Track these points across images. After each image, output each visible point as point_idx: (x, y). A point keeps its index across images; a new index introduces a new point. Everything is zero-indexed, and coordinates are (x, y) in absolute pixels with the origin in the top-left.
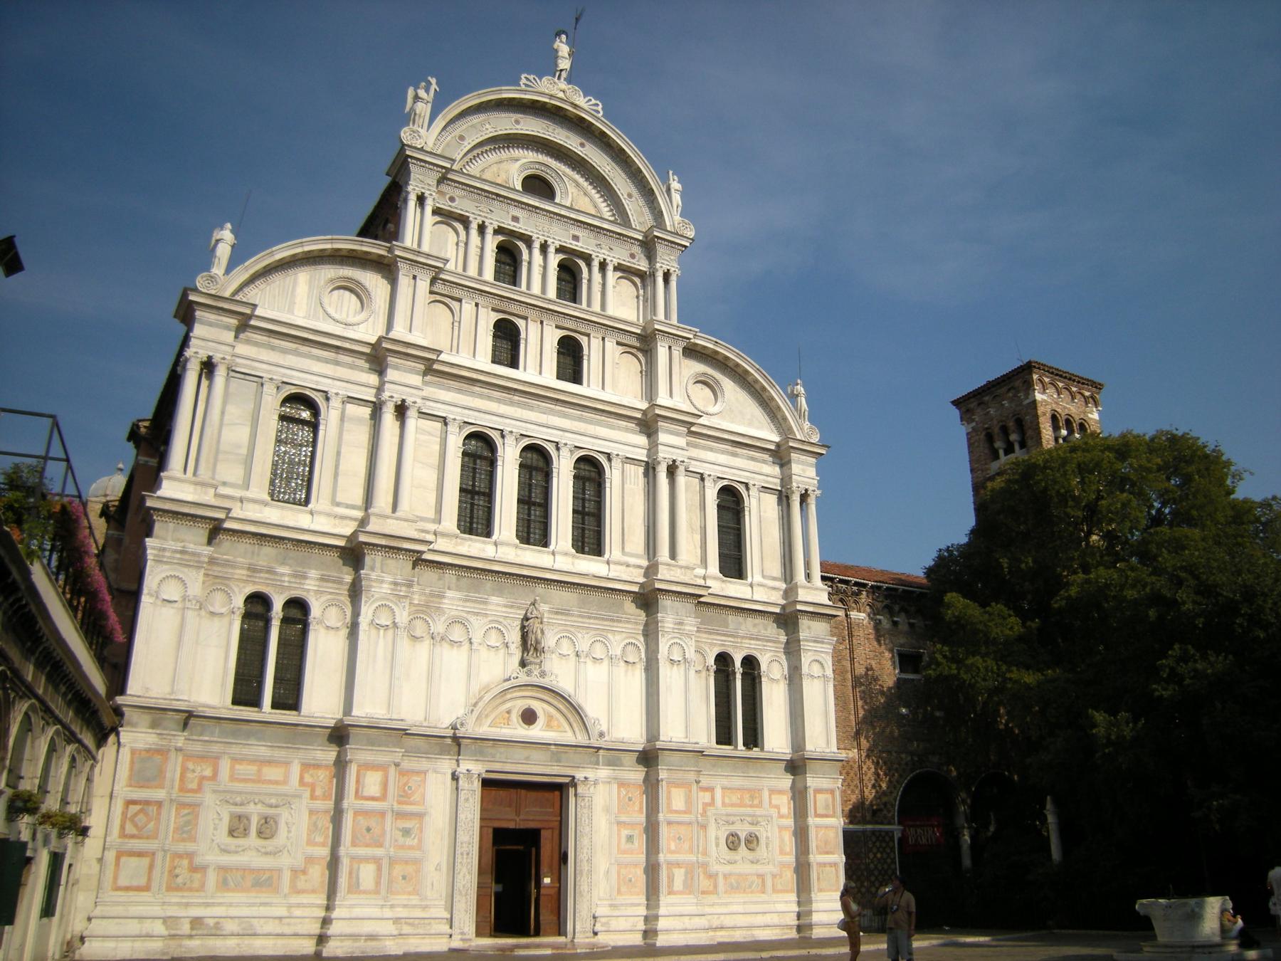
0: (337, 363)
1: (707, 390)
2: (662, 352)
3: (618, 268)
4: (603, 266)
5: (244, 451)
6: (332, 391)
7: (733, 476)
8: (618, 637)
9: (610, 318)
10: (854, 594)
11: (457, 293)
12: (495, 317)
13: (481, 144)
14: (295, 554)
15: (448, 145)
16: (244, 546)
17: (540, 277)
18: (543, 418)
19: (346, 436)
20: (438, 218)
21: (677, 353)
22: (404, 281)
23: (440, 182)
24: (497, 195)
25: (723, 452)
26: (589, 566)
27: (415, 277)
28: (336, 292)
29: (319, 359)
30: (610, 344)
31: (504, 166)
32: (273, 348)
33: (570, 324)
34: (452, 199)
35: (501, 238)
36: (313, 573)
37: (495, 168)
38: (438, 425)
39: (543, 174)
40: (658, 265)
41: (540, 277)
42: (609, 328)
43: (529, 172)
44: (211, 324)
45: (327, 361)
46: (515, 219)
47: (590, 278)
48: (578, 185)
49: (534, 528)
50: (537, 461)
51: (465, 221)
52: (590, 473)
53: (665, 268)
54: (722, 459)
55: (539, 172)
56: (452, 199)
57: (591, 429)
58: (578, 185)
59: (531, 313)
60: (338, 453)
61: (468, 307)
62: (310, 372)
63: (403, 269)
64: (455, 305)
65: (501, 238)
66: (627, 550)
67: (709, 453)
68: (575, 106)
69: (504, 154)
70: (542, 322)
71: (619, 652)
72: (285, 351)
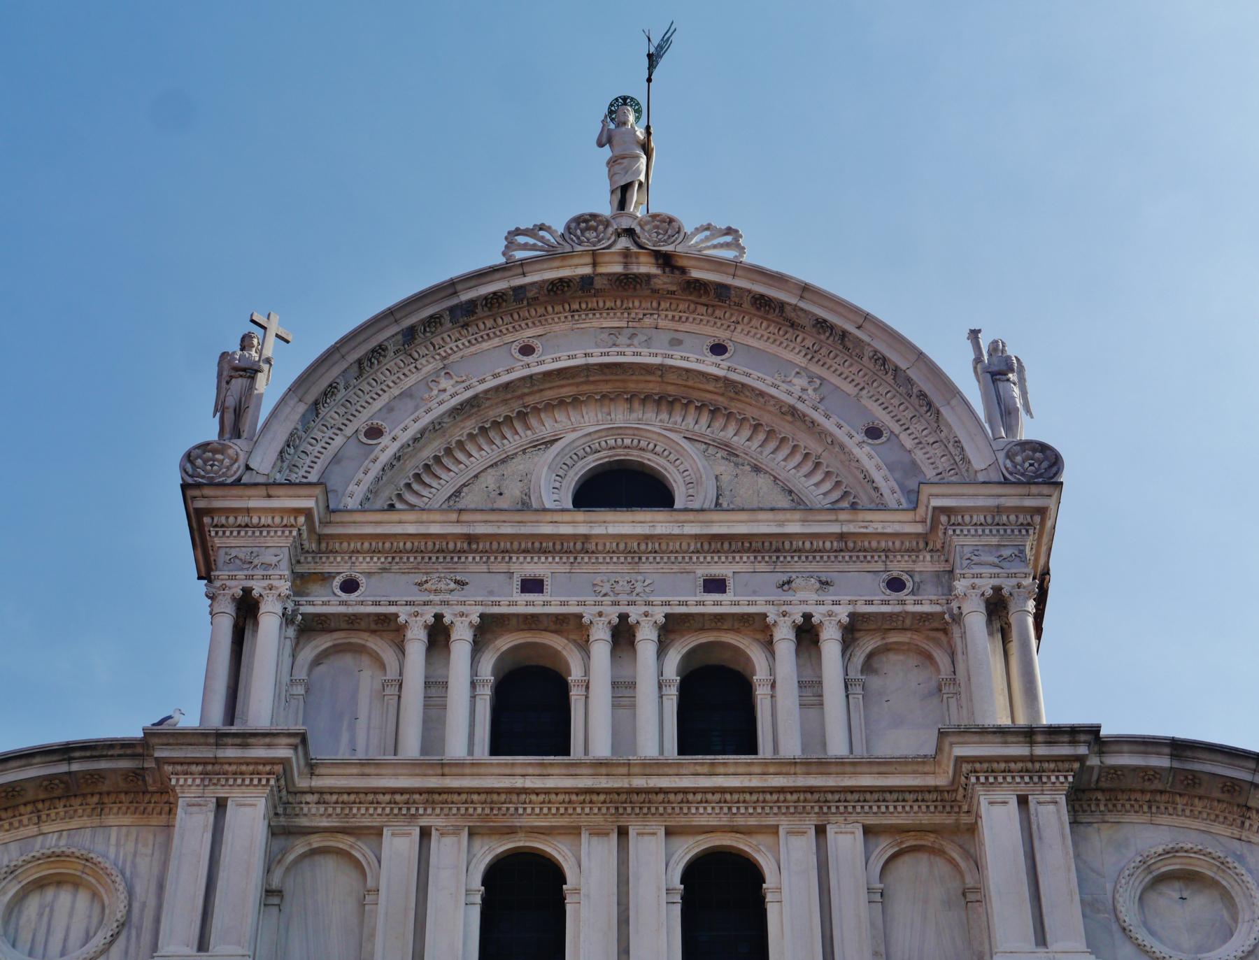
1: (1200, 904)
2: (998, 819)
3: (852, 630)
4: (807, 634)
9: (823, 765)
11: (363, 817)
12: (488, 851)
13: (436, 427)
15: (336, 459)
17: (624, 712)
20: (324, 642)
21: (1052, 813)
22: (192, 824)
23: (299, 552)
24: (470, 538)
27: (221, 805)
30: (846, 841)
31: (518, 465)
33: (704, 817)
35: (505, 643)
37: (489, 480)
39: (634, 456)
40: (960, 586)
41: (624, 712)
43: (591, 462)
46: (532, 585)
47: (775, 678)
48: (731, 453)
51: (388, 626)
53: (987, 585)
55: (621, 455)
56: (350, 586)
58: (731, 453)
61: (399, 846)
63: (188, 790)
64: (361, 850)
65: (505, 643)
68: (666, 260)
69: (514, 441)
70: (623, 833)
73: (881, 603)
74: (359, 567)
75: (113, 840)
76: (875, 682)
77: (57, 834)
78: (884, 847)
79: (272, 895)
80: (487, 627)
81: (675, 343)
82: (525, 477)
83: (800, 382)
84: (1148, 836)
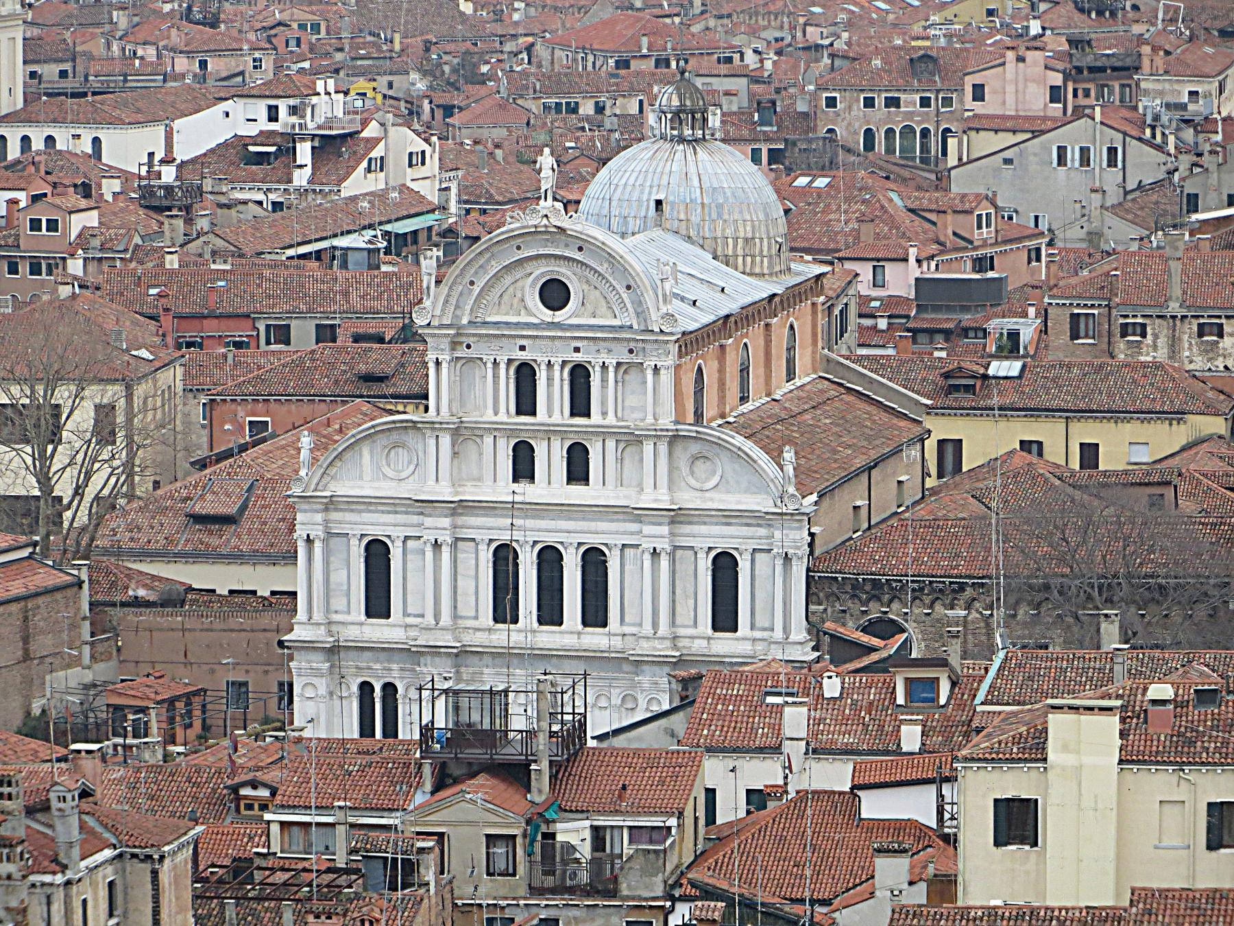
0: (396, 512)
2: (648, 447)
5: (345, 587)
6: (394, 535)
7: (722, 545)
8: (618, 691)
10: (954, 591)
12: (513, 442)
14: (382, 655)
15: (461, 294)
16: (352, 654)
18: (551, 524)
19: (409, 565)
25: (717, 524)
26: (595, 639)
28: (393, 452)
29: (383, 512)
30: (611, 444)
32: (352, 511)
34: (469, 347)
36: (395, 666)
37: (511, 290)
38: (473, 544)
42: (604, 434)
44: (305, 511)
45: (389, 512)
49: (550, 613)
50: (550, 559)
52: (594, 561)
53: (653, 364)
54: (716, 529)
57: (593, 525)
58: (587, 282)
59: (540, 435)
60: (404, 579)
61: (489, 440)
62: (379, 525)
64: (478, 440)
66: (627, 619)
67: (703, 527)
71: (619, 702)
72: (360, 511)
73: (626, 358)
74: (471, 340)
75: (411, 438)
76: (627, 377)
77: (395, 436)
78: (622, 446)
79: (455, 454)
80: (510, 361)
81: (567, 245)
82: (522, 289)
83: (606, 265)
84: (695, 448)
